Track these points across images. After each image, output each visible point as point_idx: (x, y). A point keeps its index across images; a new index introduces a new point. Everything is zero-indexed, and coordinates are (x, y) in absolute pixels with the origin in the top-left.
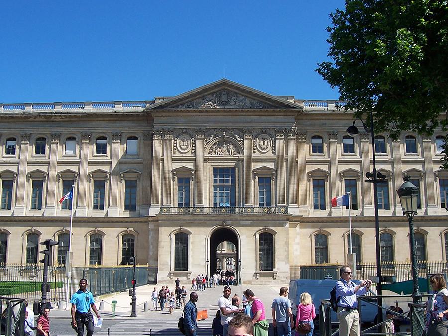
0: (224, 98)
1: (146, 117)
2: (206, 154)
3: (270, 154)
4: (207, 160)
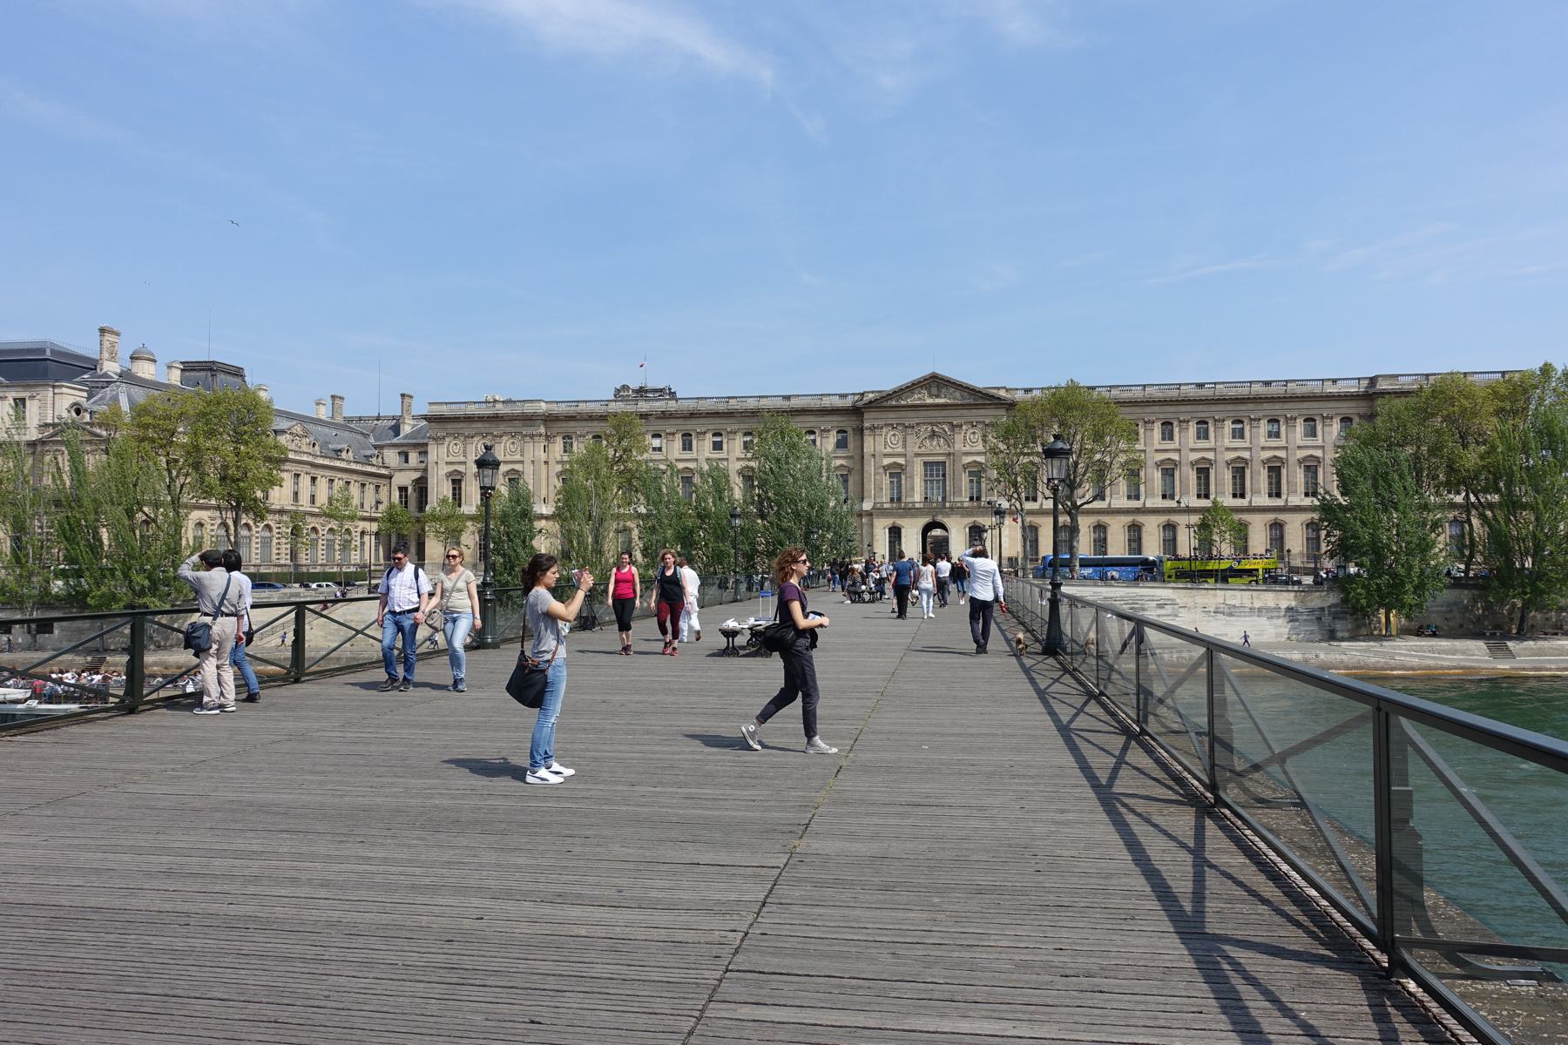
0: (934, 391)
1: (856, 411)
2: (916, 450)
3: (980, 448)
4: (917, 455)
